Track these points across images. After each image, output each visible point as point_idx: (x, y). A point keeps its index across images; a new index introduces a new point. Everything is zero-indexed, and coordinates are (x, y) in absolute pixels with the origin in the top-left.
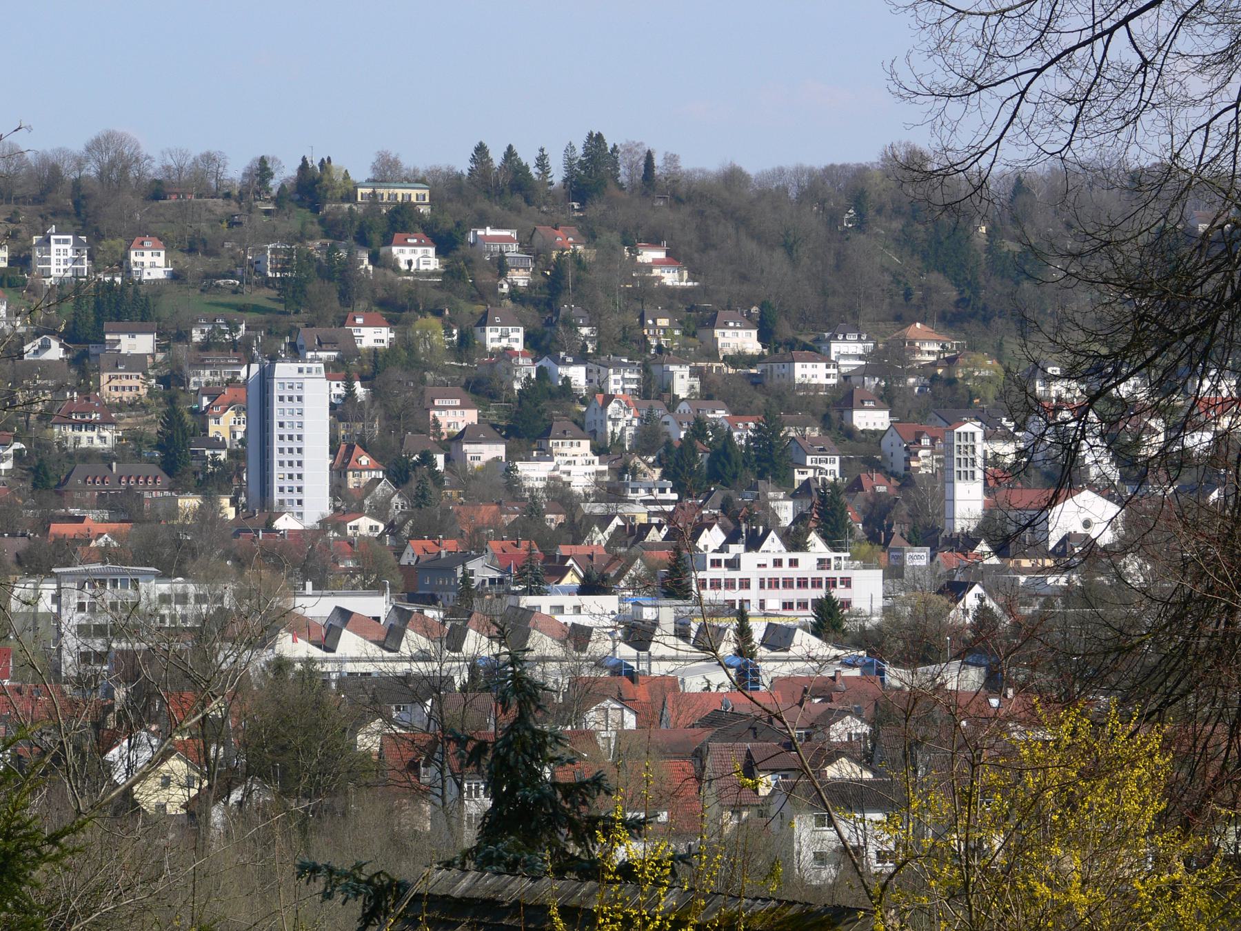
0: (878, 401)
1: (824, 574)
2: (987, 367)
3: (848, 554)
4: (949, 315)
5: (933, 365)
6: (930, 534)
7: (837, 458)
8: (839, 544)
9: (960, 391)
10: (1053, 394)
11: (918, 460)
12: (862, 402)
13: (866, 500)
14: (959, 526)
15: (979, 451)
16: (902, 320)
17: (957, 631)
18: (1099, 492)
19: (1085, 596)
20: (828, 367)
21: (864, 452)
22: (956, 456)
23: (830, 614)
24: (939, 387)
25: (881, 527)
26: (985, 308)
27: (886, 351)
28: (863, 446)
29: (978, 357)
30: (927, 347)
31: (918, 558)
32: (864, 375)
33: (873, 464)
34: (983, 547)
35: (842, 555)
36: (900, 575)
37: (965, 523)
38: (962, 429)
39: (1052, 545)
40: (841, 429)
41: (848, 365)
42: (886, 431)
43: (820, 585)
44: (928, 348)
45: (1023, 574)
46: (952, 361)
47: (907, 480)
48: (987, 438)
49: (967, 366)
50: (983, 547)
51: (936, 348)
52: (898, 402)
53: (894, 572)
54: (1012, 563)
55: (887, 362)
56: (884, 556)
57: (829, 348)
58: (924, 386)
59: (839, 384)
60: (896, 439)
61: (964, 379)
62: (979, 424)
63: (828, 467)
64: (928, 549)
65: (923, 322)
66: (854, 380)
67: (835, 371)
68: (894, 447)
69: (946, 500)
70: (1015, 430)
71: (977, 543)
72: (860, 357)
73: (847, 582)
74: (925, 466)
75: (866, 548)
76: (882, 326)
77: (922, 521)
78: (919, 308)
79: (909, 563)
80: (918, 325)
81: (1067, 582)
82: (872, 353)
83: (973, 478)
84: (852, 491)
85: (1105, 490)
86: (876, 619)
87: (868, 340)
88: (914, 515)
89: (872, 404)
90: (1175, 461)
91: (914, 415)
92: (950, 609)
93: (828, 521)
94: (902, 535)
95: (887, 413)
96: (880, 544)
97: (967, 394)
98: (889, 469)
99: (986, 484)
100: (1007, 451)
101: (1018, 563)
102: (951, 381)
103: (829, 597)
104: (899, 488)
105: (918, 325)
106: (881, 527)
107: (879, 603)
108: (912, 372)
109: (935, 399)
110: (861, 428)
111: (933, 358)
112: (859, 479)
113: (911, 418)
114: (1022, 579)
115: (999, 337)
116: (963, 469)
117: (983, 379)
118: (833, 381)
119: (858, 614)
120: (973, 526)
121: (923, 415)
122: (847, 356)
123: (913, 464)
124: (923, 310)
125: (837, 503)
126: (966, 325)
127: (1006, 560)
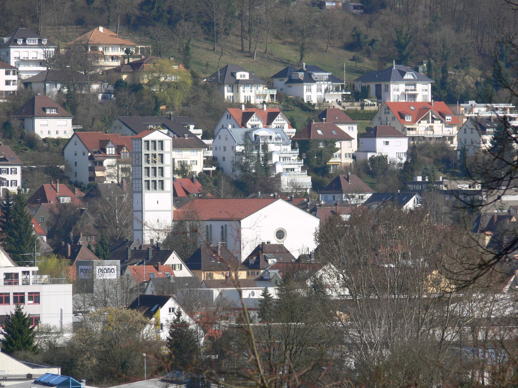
0: (60, 108)
1: (11, 290)
2: (174, 73)
3: (36, 269)
4: (133, 18)
5: (118, 70)
6: (118, 246)
7: (19, 168)
8: (24, 258)
9: (146, 98)
10: (242, 100)
11: (104, 170)
12: (44, 109)
13: (51, 211)
14: (148, 237)
15: (167, 160)
16: (84, 24)
17: (152, 346)
18: (290, 201)
19: (284, 309)
20: (7, 73)
21: (47, 162)
22: (144, 165)
23: (20, 332)
24: (124, 93)
25: (67, 240)
26: (170, 12)
27: (68, 55)
28: (46, 155)
29: (164, 62)
30: (110, 52)
31: (108, 271)
32: (45, 82)
33: (56, 175)
34: (173, 259)
35: (30, 269)
36: (90, 290)
37: (154, 234)
38: (150, 137)
39: (244, 256)
40: (22, 137)
41: (29, 71)
42: (70, 140)
43: (7, 301)
44: (112, 52)
45: (217, 287)
46: (136, 66)
47: (92, 190)
48: (176, 146)
49: (153, 72)
50: (173, 259)
51: (120, 53)
52: (80, 109)
53: (83, 287)
54: (203, 276)
55: (69, 68)
56: (72, 270)
57: (8, 54)
58: (109, 92)
59: (19, 91)
60: (80, 148)
61: (151, 84)
62: (166, 131)
63: (9, 177)
64: (118, 262)
65: (106, 26)
66: (35, 87)
67: (15, 77)
68: (78, 157)
69: (134, 213)
70: (203, 138)
71: (166, 255)
72: (41, 63)
73: (35, 297)
74: (110, 176)
75: (53, 261)
76: (64, 29)
77: (109, 232)
78: (101, 11)
79: (99, 276)
80: (101, 29)
81: (264, 294)
82: (53, 59)
83: (162, 188)
84: (36, 202)
85: (298, 199)
86: (68, 336)
87: (50, 44)
88: (100, 226)
89: (54, 112)
90: (372, 169)
91: (98, 123)
92: (145, 324)
93: (11, 234)
94: (89, 247)
95: (70, 121)
96: (67, 257)
97: (153, 102)
98: (73, 179)
99: (175, 194)
100: (196, 160)
101: (211, 276)
102: (136, 88)
103: (18, 314)
104: (84, 199)
105: (101, 29)
106: (67, 240)
107: (69, 319)
108: (95, 79)
109: (120, 106)
110: (43, 136)
111: (117, 63)
112: (42, 189)
113: (95, 126)
114: (216, 293)
115: (185, 41)
116: (151, 178)
117: (169, 84)
118: (13, 88)
119: (48, 331)
120: (163, 237)
121: (107, 123)
122: (26, 62)
123: (98, 174)
124: (107, 14)
125: (21, 214)
126: (151, 29)
127: (197, 272)
